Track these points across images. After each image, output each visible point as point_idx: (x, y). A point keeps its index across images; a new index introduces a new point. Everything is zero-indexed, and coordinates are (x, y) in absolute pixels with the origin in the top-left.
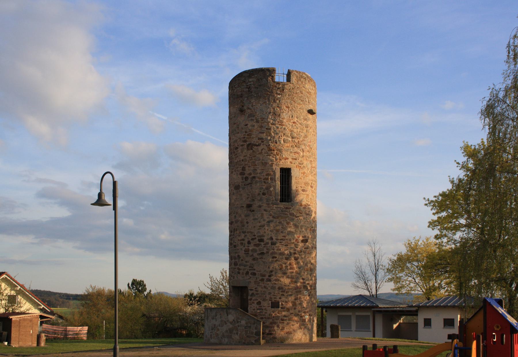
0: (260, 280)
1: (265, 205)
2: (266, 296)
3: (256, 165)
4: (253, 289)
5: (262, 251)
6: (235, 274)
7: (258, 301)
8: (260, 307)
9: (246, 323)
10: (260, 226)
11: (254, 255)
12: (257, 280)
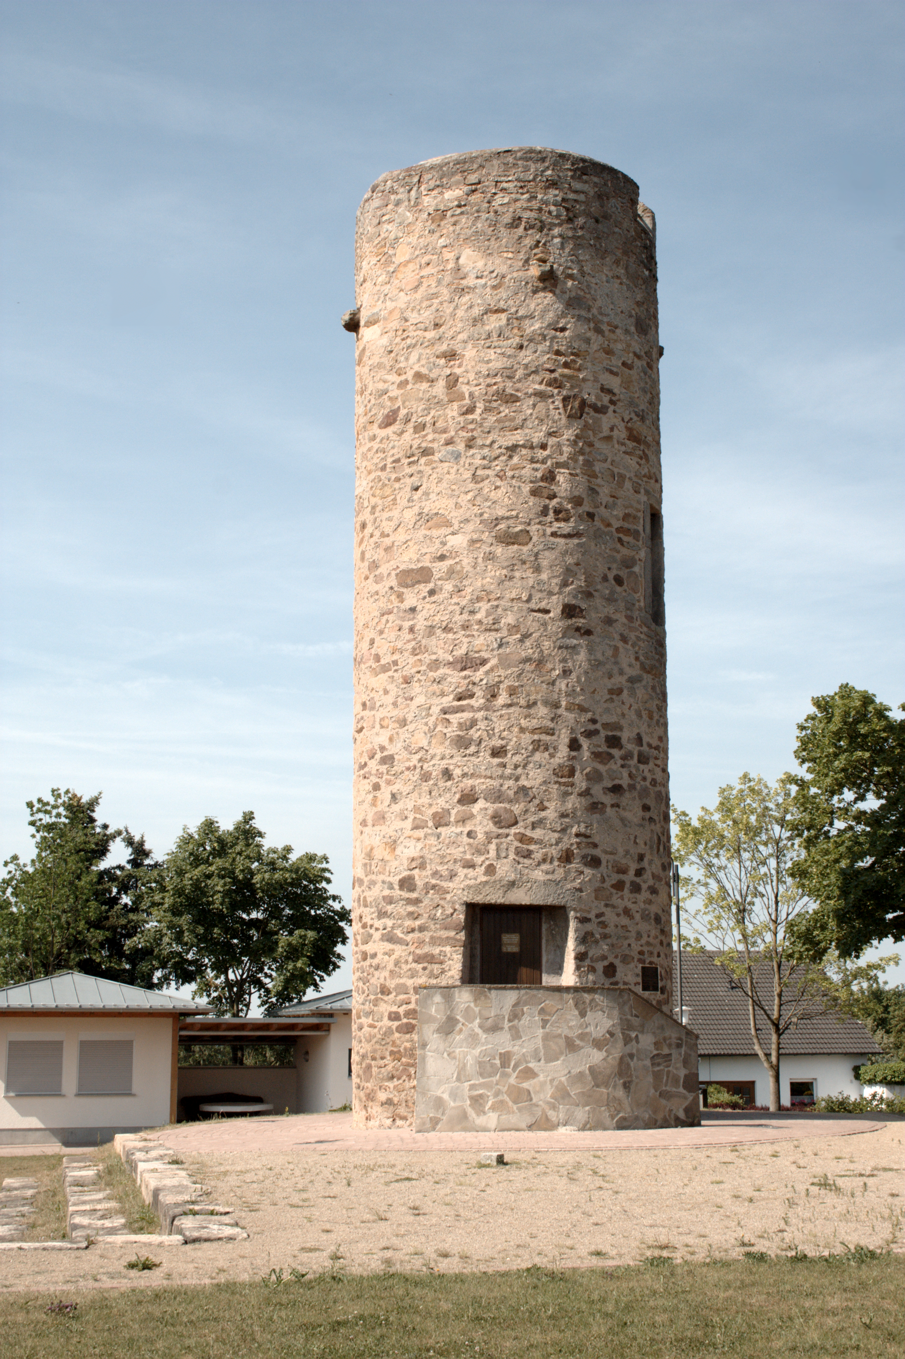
0: (613, 886)
1: (621, 618)
2: (629, 945)
3: (596, 477)
4: (589, 916)
5: (617, 782)
6: (498, 857)
7: (606, 963)
8: (611, 984)
9: (655, 1044)
10: (611, 692)
11: (592, 792)
12: (605, 885)
